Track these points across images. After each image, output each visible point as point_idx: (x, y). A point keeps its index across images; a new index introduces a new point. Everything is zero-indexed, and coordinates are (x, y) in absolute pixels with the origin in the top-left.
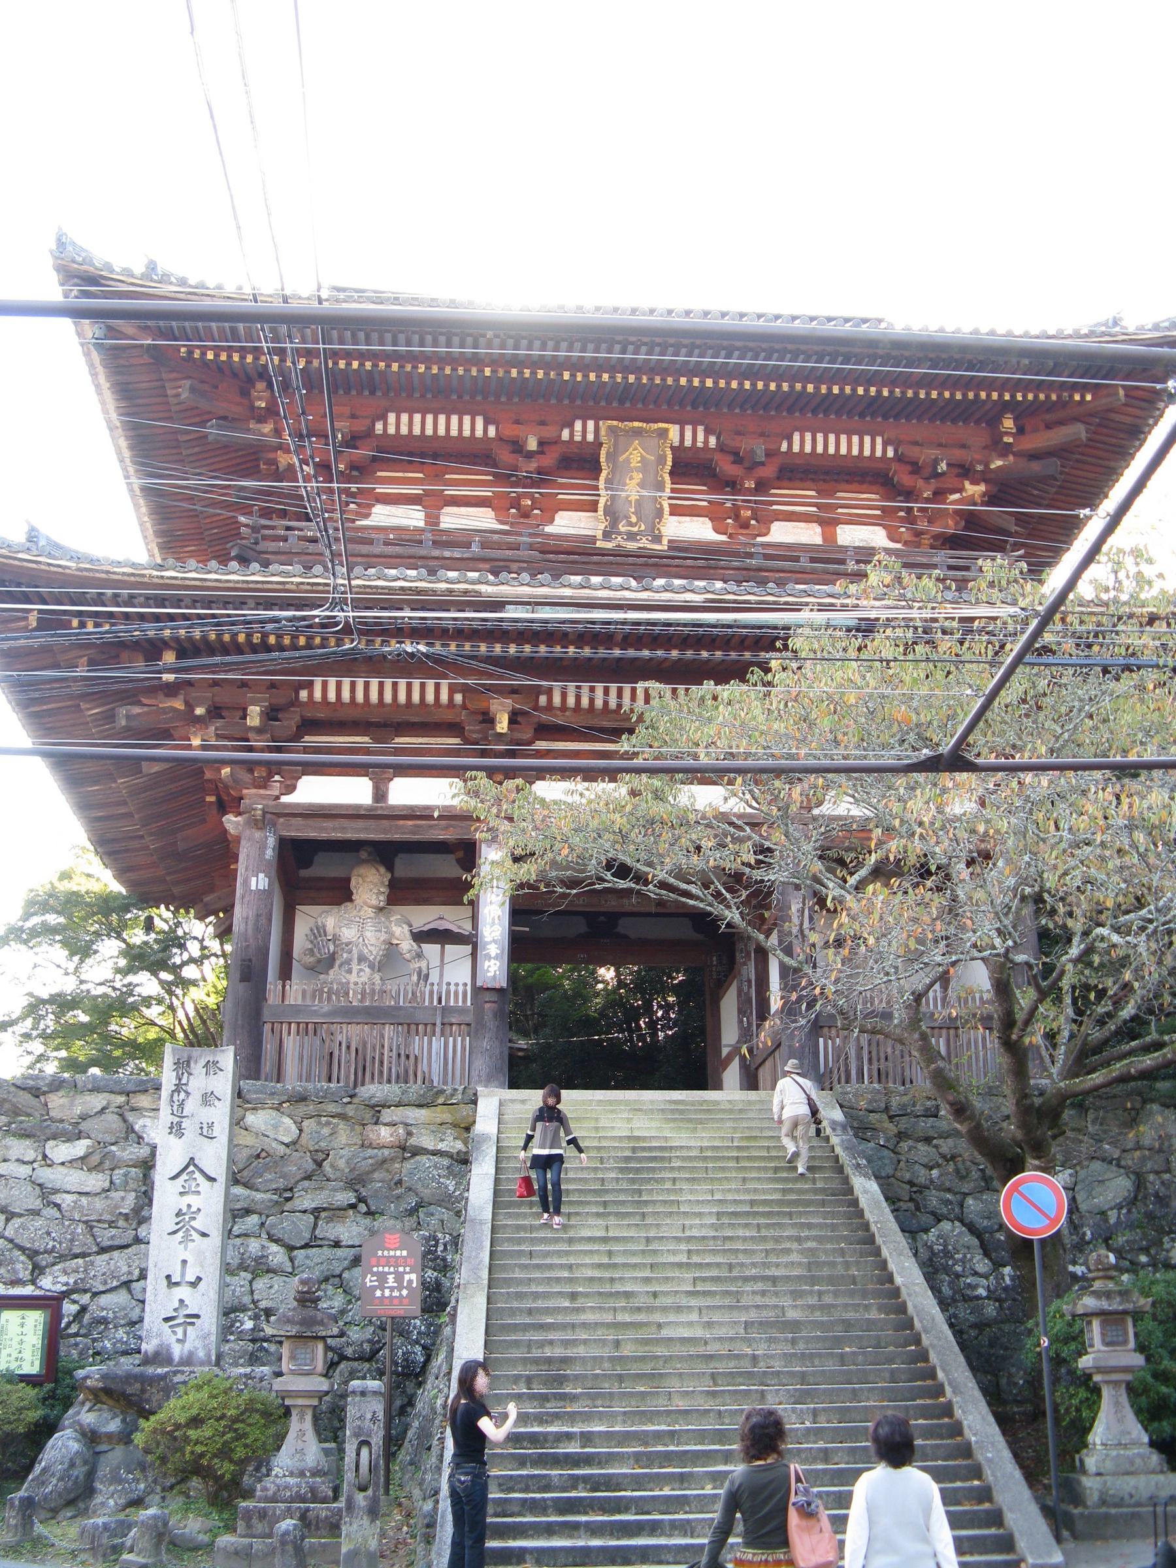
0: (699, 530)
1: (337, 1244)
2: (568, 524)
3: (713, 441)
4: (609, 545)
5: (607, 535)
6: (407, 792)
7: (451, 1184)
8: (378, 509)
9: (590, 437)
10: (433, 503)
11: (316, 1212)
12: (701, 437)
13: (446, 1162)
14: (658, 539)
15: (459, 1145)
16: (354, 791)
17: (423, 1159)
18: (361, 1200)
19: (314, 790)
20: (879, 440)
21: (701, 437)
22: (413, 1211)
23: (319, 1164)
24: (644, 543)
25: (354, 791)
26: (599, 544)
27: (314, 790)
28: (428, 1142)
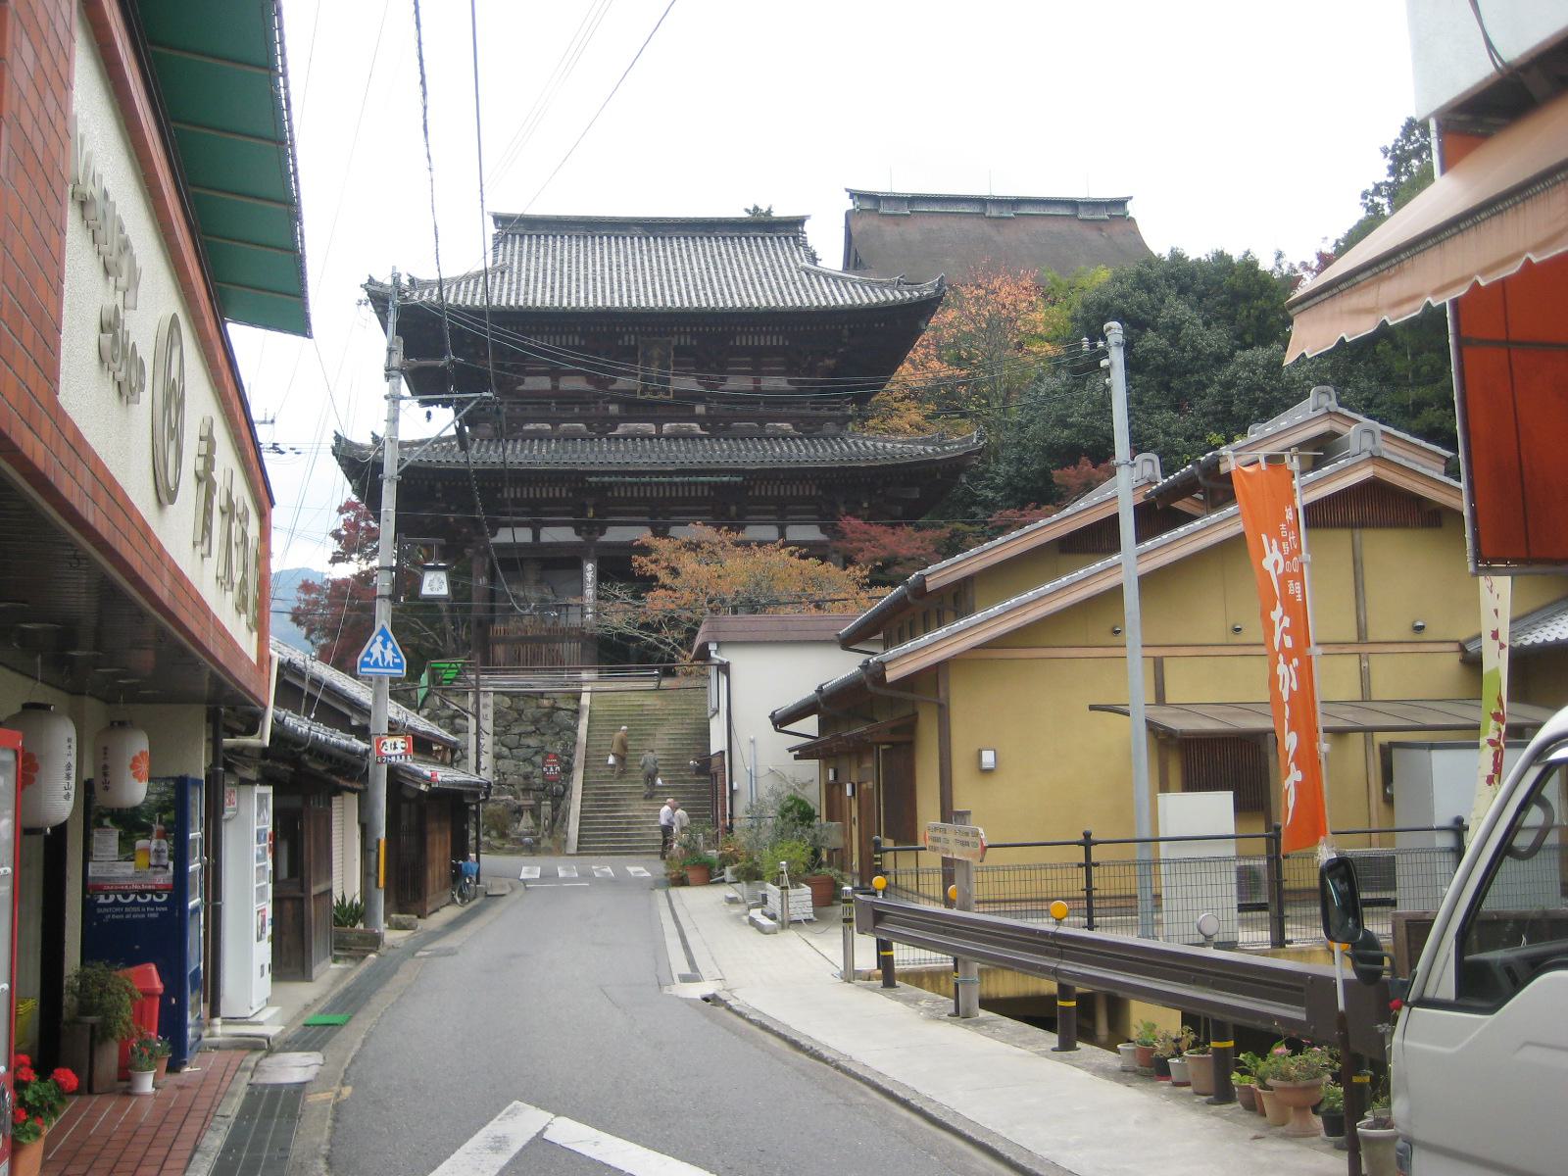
0: (689, 384)
1: (529, 747)
2: (623, 383)
3: (695, 343)
4: (643, 397)
5: (642, 393)
6: (549, 535)
7: (572, 722)
8: (528, 380)
9: (633, 343)
10: (555, 374)
11: (520, 734)
12: (688, 340)
13: (570, 713)
14: (668, 393)
15: (575, 707)
16: (524, 535)
17: (562, 713)
18: (538, 729)
19: (504, 536)
20: (781, 338)
21: (688, 340)
22: (558, 733)
23: (520, 715)
24: (661, 396)
25: (524, 535)
26: (639, 396)
27: (504, 536)
28: (562, 706)
